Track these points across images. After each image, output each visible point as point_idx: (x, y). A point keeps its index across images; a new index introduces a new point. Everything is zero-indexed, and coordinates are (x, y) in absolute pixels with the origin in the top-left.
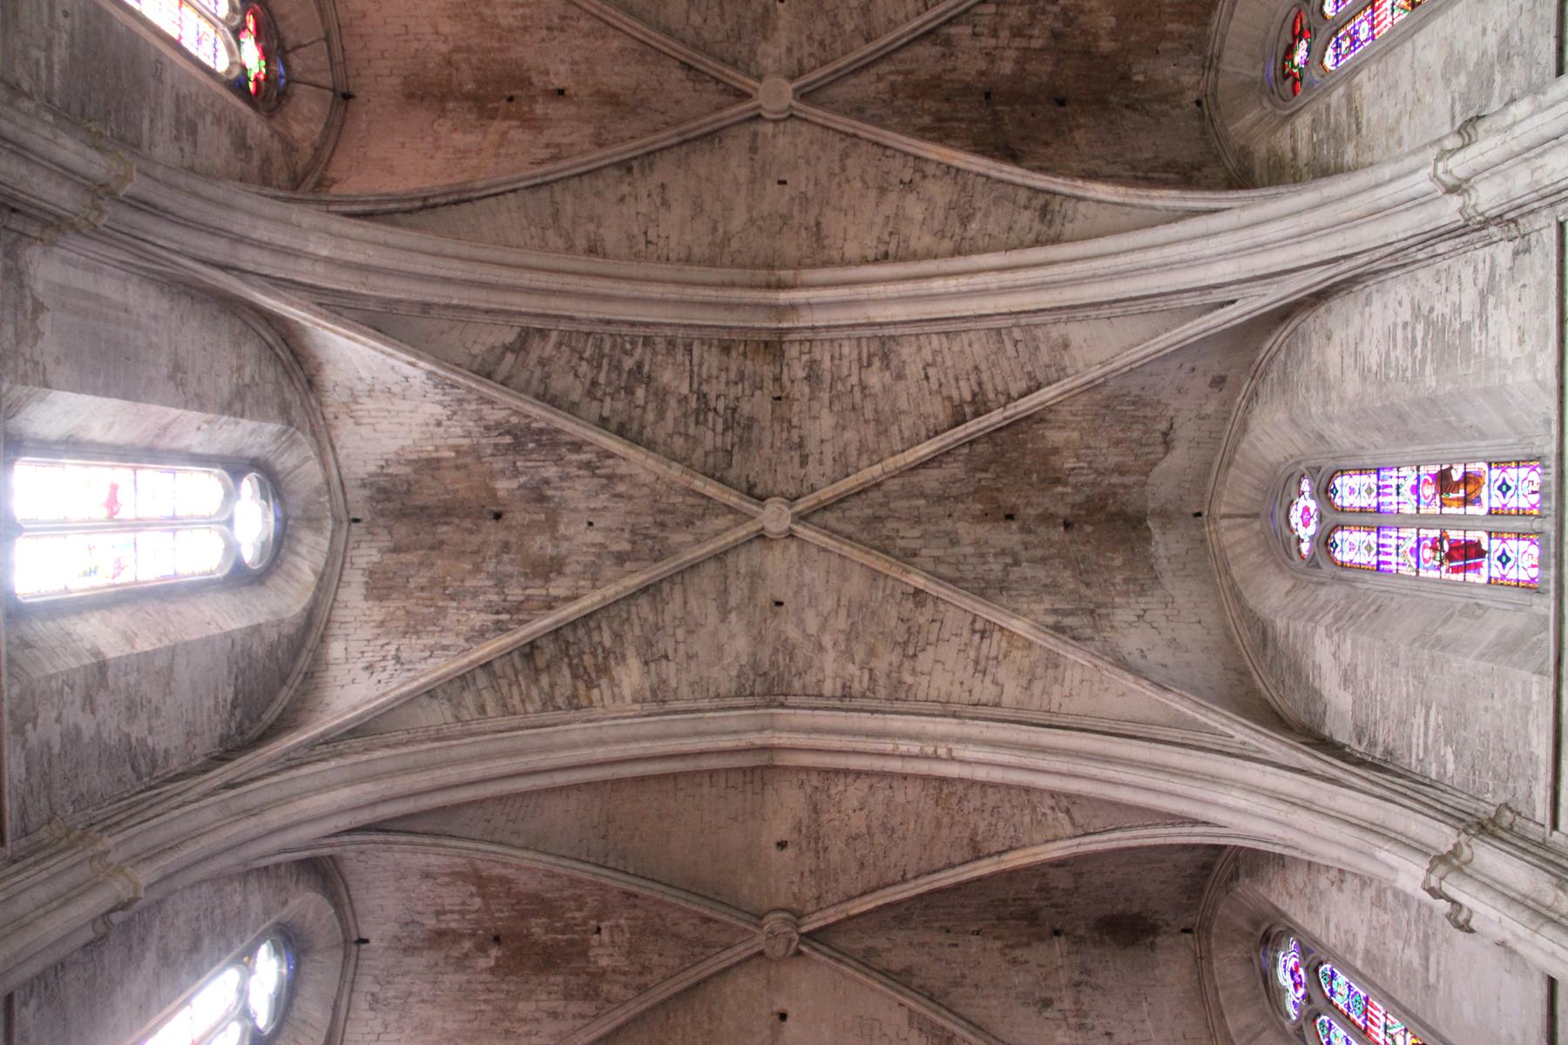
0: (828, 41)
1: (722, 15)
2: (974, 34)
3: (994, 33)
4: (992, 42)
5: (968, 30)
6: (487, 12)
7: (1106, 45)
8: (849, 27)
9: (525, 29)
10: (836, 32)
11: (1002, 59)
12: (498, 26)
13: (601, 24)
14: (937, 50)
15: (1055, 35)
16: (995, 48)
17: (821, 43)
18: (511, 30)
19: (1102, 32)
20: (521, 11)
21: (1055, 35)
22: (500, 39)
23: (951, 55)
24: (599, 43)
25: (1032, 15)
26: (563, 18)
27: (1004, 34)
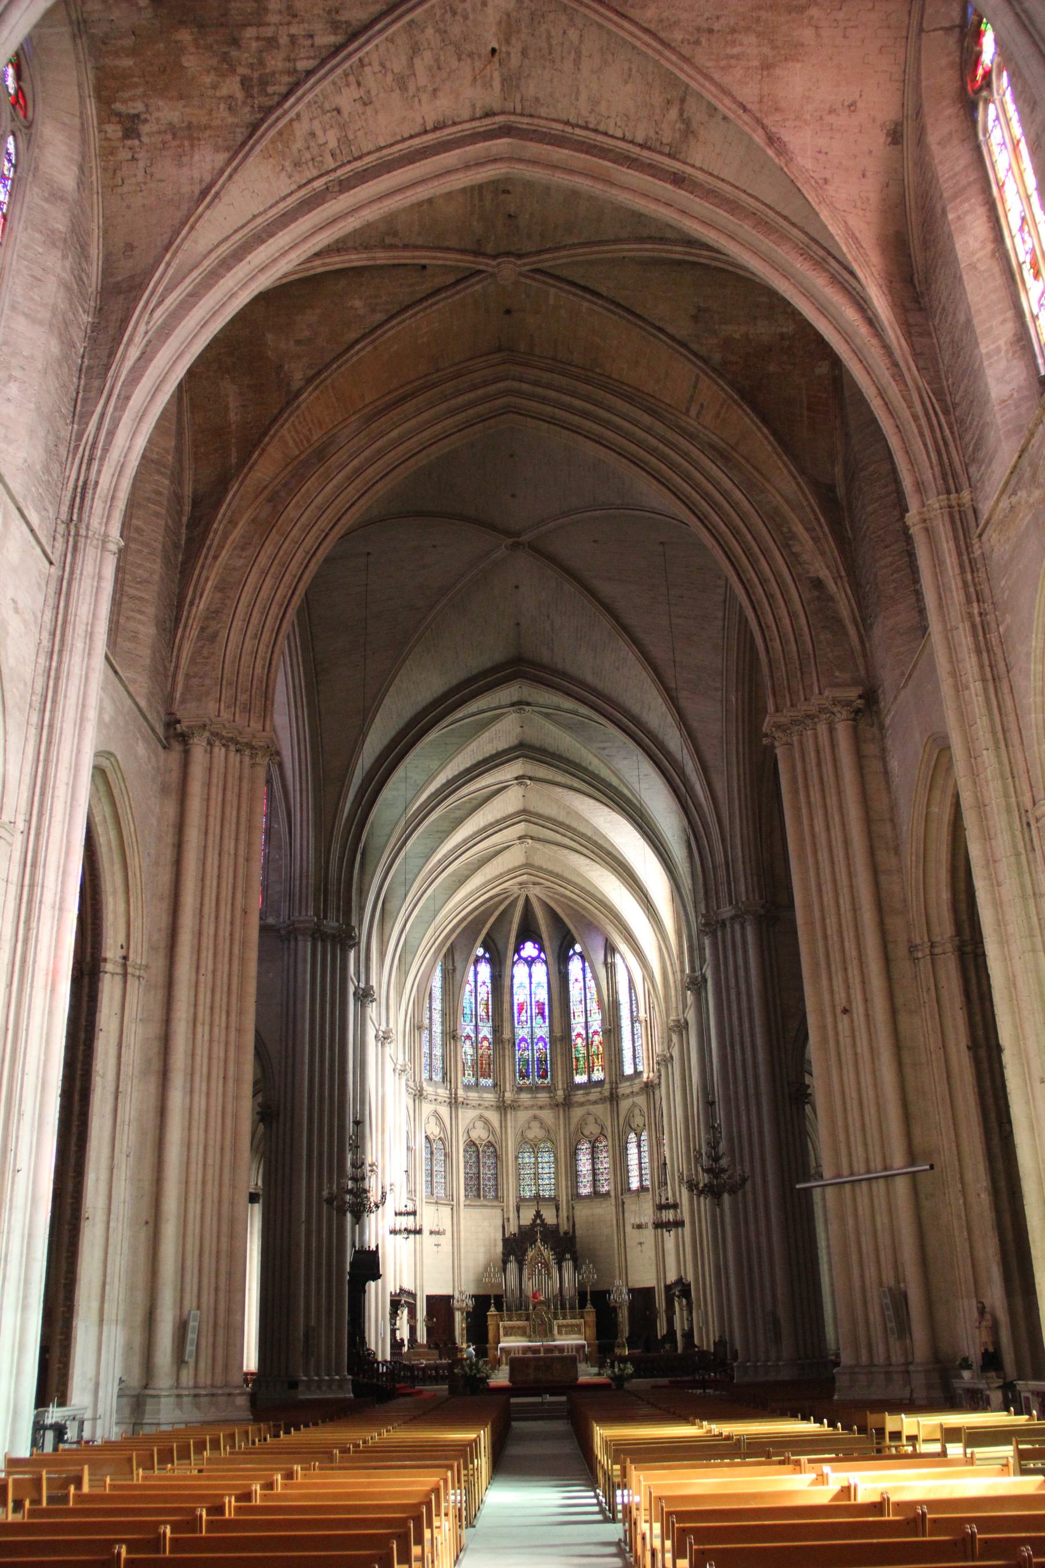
0: (448, 16)
1: (549, 37)
2: (311, 36)
3: (293, 39)
4: (293, 30)
5: (320, 40)
6: (766, 50)
7: (185, 36)
8: (430, 31)
9: (733, 31)
10: (441, 25)
11: (280, 12)
12: (759, 35)
13: (662, 35)
14: (345, 16)
15: (235, 42)
16: (289, 24)
17: (454, 13)
18: (748, 29)
19: (192, 50)
20: (736, 50)
21: (235, 42)
22: (758, 19)
23: (329, 12)
24: (665, 14)
25: (262, 63)
26: (698, 42)
27: (284, 40)
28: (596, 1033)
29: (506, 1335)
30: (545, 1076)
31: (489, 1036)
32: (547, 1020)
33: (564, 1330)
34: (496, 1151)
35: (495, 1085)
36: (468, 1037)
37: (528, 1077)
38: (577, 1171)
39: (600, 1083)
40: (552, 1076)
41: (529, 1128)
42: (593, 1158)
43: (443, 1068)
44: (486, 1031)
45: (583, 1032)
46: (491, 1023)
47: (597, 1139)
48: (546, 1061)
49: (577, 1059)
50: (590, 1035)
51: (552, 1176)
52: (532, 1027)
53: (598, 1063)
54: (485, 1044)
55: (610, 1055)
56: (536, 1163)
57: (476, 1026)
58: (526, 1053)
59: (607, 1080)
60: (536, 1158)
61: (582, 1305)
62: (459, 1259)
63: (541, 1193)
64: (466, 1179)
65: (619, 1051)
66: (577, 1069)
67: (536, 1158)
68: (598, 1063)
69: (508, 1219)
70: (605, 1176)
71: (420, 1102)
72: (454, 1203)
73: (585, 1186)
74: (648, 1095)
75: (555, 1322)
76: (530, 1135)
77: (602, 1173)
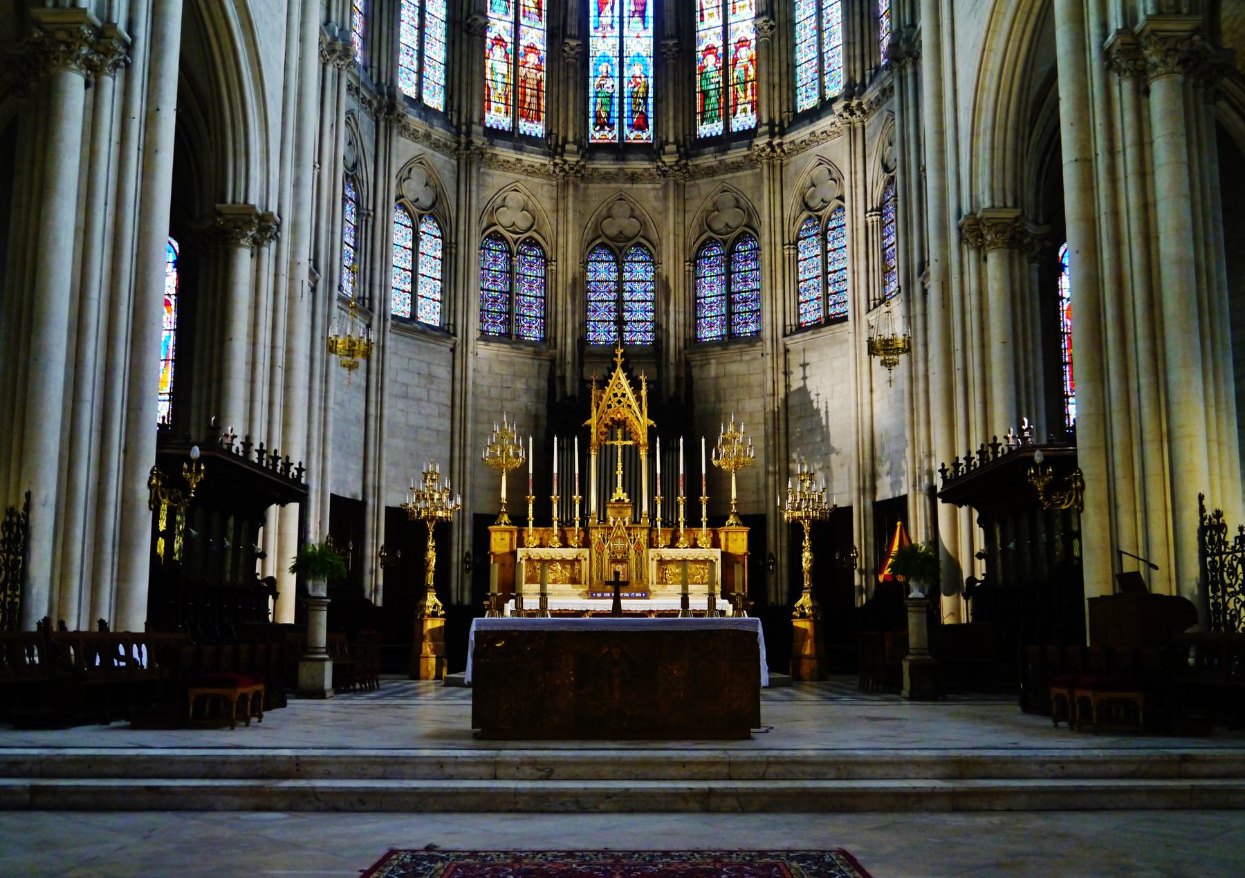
28: (743, 43)
29: (531, 580)
30: (641, 126)
31: (541, 47)
32: (650, 25)
33: (673, 569)
34: (544, 257)
35: (549, 133)
36: (499, 41)
37: (611, 126)
38: (697, 298)
39: (748, 135)
40: (655, 124)
41: (609, 216)
42: (729, 273)
43: (446, 87)
44: (535, 34)
45: (718, 43)
46: (543, 25)
47: (738, 240)
48: (645, 98)
49: (705, 94)
50: (732, 48)
51: (650, 306)
52: (621, 37)
53: (745, 97)
54: (532, 59)
55: (770, 74)
56: (620, 282)
57: (517, 24)
58: (609, 82)
59: (765, 120)
60: (620, 271)
61: (717, 521)
62: (463, 448)
63: (627, 337)
64: (484, 300)
65: (792, 66)
66: (703, 112)
67: (620, 271)
68: (745, 97)
69: (563, 378)
70: (751, 306)
71: (388, 129)
72: (459, 339)
73: (711, 325)
74: (852, 131)
75: (652, 552)
76: (611, 229)
77: (745, 300)
